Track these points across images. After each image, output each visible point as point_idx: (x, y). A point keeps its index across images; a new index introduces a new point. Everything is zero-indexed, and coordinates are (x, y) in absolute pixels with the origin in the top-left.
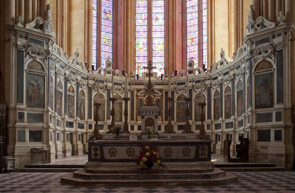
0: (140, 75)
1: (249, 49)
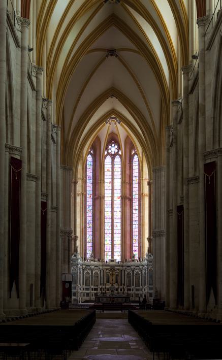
0: (108, 261)
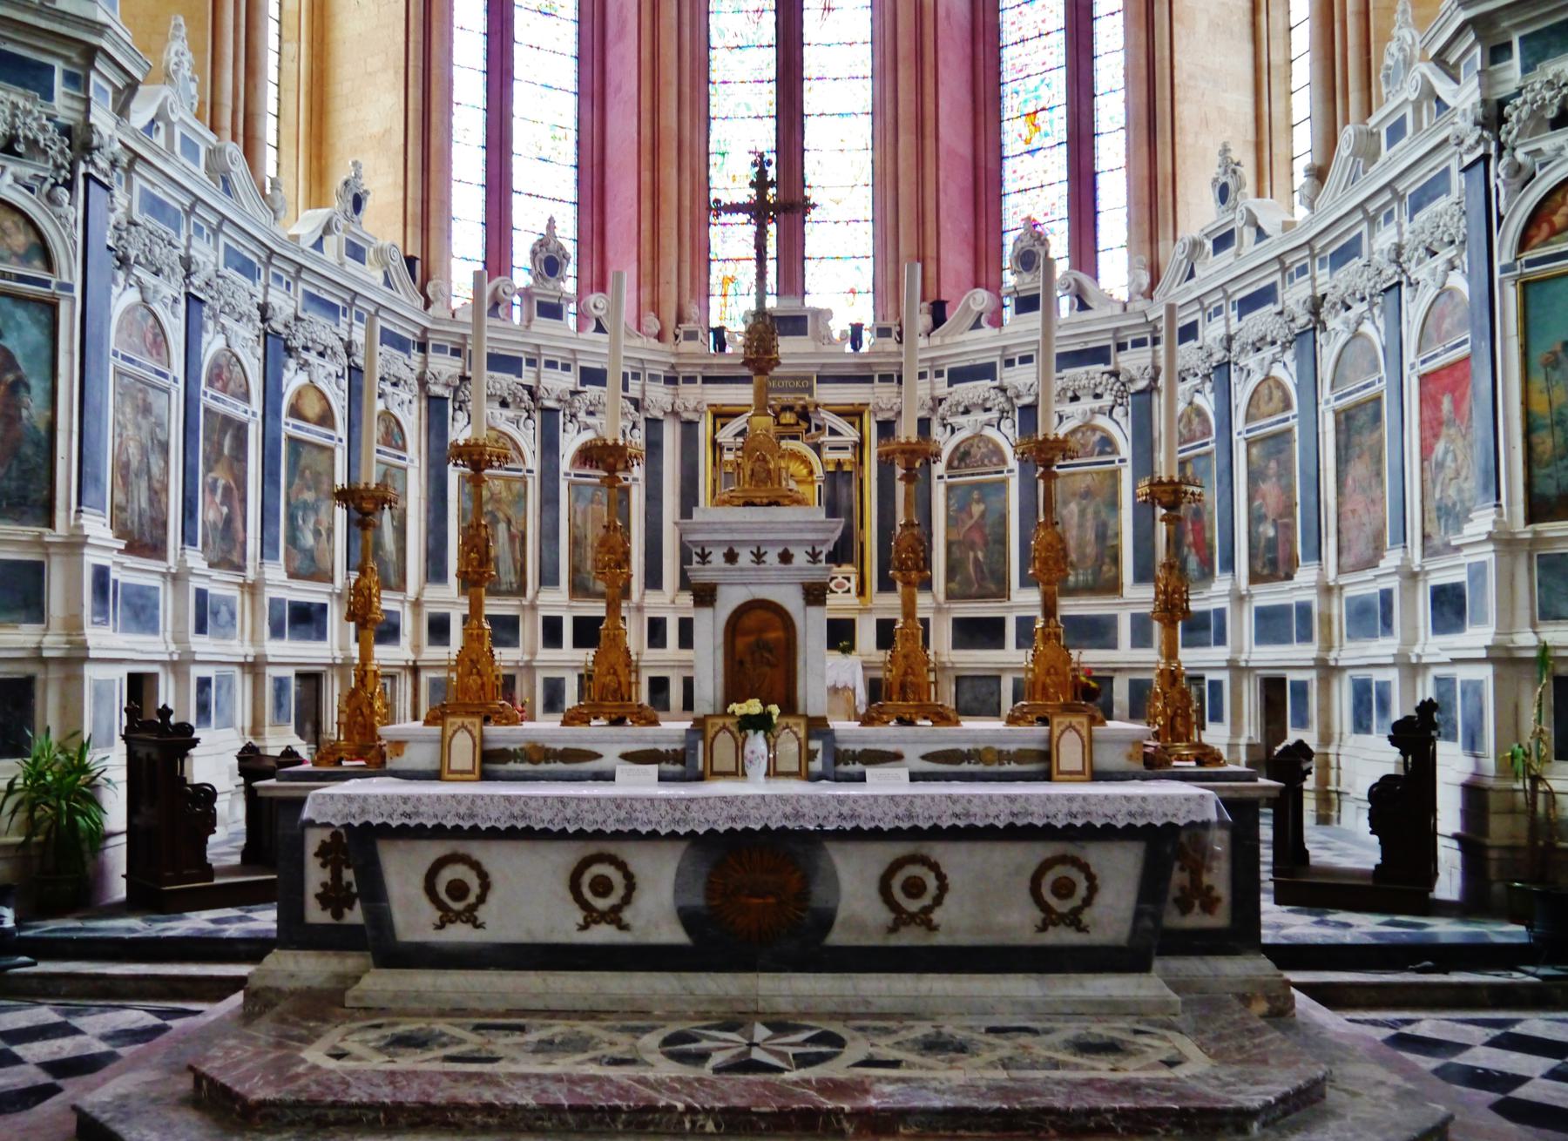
1: (1465, 96)
